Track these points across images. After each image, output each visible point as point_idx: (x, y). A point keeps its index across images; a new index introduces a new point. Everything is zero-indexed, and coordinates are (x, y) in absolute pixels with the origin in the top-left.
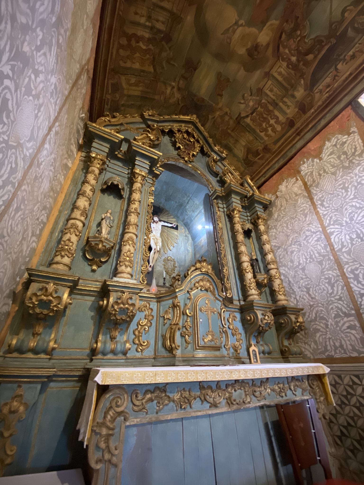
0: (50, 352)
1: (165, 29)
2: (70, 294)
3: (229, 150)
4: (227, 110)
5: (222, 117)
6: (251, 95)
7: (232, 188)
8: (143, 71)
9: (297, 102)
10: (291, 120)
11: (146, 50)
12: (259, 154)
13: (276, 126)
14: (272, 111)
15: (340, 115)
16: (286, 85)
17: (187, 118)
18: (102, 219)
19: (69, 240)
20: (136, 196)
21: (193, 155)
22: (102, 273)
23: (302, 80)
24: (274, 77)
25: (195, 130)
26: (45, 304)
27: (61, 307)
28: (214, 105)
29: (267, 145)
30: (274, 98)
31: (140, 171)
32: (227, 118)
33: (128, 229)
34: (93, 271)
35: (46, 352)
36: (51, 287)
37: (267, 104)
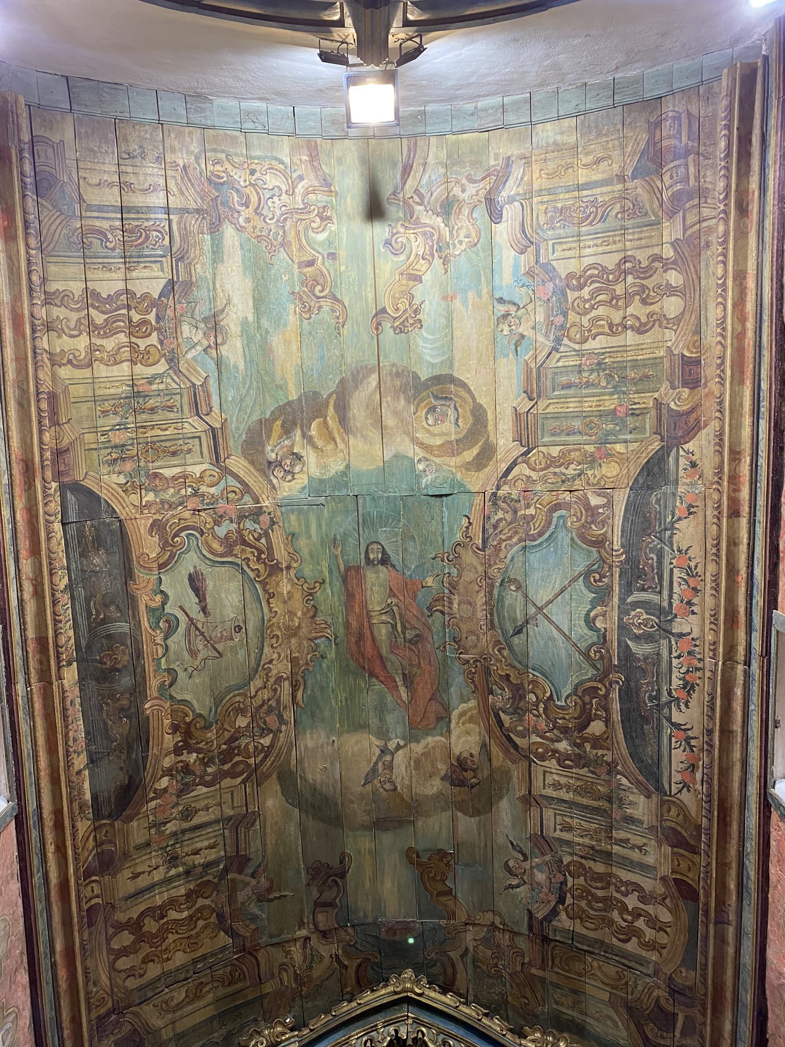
1: (222, 853)
5: (485, 941)
6: (526, 858)
8: (204, 958)
9: (651, 828)
10: (675, 880)
11: (191, 917)
12: (675, 1015)
13: (650, 909)
14: (610, 875)
15: (773, 843)
16: (595, 804)
17: (383, 994)
23: (619, 777)
25: (425, 1017)
28: (443, 922)
29: (670, 978)
30: (587, 841)
32: (504, 940)
37: (581, 864)
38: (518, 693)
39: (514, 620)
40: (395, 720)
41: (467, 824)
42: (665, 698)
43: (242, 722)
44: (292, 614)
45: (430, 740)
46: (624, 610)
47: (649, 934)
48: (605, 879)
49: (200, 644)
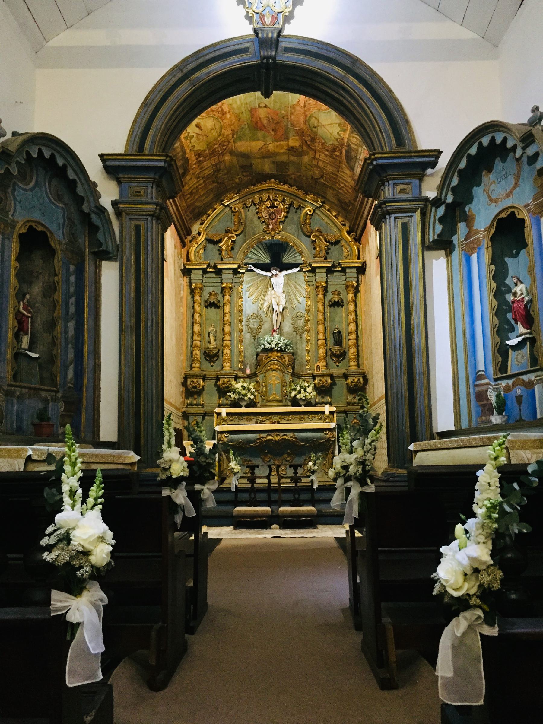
0: (202, 405)
2: (203, 381)
3: (323, 197)
4: (299, 174)
5: (298, 177)
7: (313, 265)
13: (348, 189)
17: (264, 186)
18: (209, 333)
19: (196, 354)
20: (227, 309)
21: (281, 221)
22: (216, 366)
24: (321, 160)
25: (277, 192)
26: (195, 387)
27: (201, 387)
31: (227, 283)
33: (225, 337)
34: (212, 366)
35: (200, 405)
36: (195, 380)
38: (313, 140)
39: (314, 124)
40: (269, 140)
41: (292, 158)
42: (358, 158)
43: (216, 146)
44: (231, 121)
45: (282, 143)
46: (349, 136)
47: (346, 192)
48: (336, 179)
49: (201, 137)
